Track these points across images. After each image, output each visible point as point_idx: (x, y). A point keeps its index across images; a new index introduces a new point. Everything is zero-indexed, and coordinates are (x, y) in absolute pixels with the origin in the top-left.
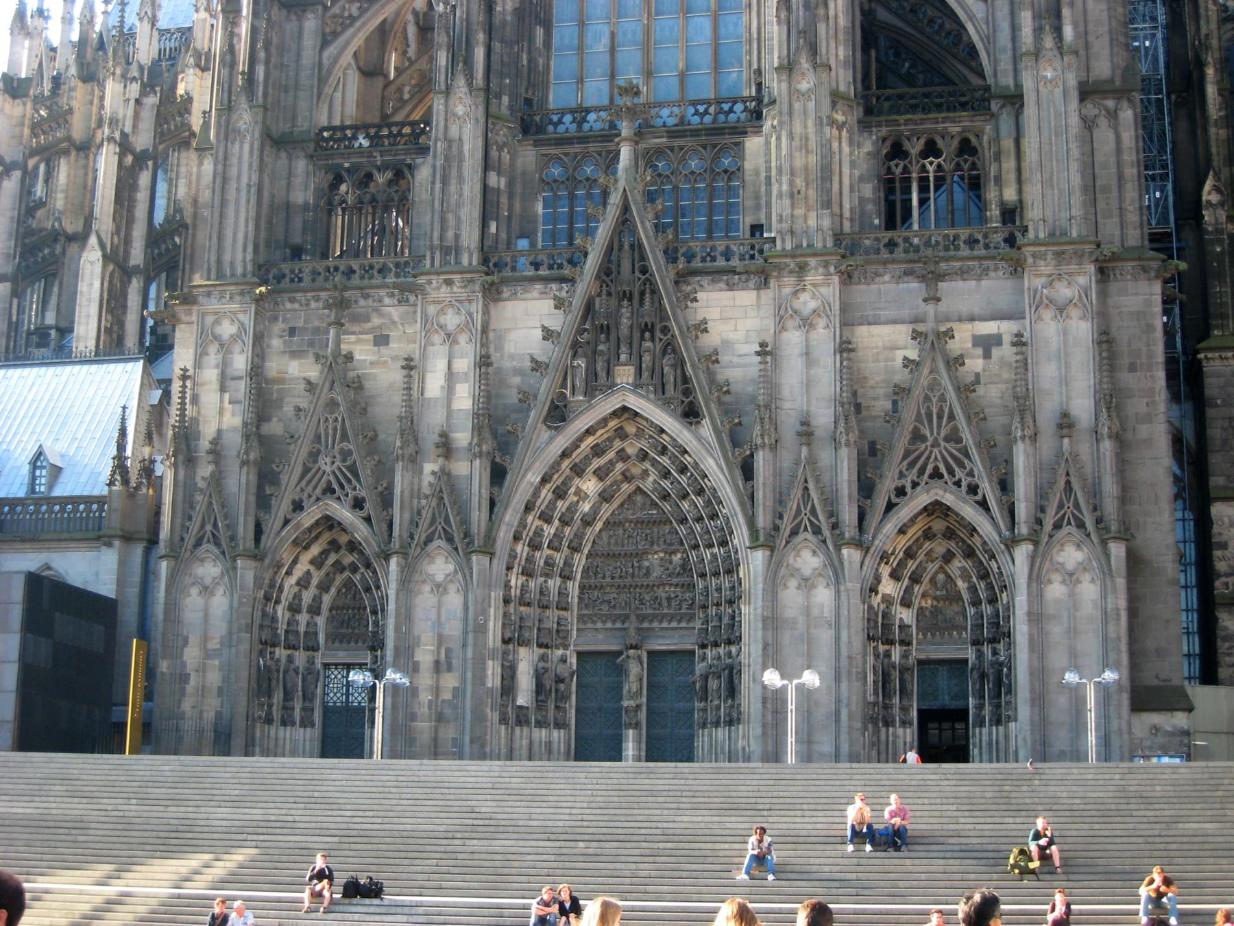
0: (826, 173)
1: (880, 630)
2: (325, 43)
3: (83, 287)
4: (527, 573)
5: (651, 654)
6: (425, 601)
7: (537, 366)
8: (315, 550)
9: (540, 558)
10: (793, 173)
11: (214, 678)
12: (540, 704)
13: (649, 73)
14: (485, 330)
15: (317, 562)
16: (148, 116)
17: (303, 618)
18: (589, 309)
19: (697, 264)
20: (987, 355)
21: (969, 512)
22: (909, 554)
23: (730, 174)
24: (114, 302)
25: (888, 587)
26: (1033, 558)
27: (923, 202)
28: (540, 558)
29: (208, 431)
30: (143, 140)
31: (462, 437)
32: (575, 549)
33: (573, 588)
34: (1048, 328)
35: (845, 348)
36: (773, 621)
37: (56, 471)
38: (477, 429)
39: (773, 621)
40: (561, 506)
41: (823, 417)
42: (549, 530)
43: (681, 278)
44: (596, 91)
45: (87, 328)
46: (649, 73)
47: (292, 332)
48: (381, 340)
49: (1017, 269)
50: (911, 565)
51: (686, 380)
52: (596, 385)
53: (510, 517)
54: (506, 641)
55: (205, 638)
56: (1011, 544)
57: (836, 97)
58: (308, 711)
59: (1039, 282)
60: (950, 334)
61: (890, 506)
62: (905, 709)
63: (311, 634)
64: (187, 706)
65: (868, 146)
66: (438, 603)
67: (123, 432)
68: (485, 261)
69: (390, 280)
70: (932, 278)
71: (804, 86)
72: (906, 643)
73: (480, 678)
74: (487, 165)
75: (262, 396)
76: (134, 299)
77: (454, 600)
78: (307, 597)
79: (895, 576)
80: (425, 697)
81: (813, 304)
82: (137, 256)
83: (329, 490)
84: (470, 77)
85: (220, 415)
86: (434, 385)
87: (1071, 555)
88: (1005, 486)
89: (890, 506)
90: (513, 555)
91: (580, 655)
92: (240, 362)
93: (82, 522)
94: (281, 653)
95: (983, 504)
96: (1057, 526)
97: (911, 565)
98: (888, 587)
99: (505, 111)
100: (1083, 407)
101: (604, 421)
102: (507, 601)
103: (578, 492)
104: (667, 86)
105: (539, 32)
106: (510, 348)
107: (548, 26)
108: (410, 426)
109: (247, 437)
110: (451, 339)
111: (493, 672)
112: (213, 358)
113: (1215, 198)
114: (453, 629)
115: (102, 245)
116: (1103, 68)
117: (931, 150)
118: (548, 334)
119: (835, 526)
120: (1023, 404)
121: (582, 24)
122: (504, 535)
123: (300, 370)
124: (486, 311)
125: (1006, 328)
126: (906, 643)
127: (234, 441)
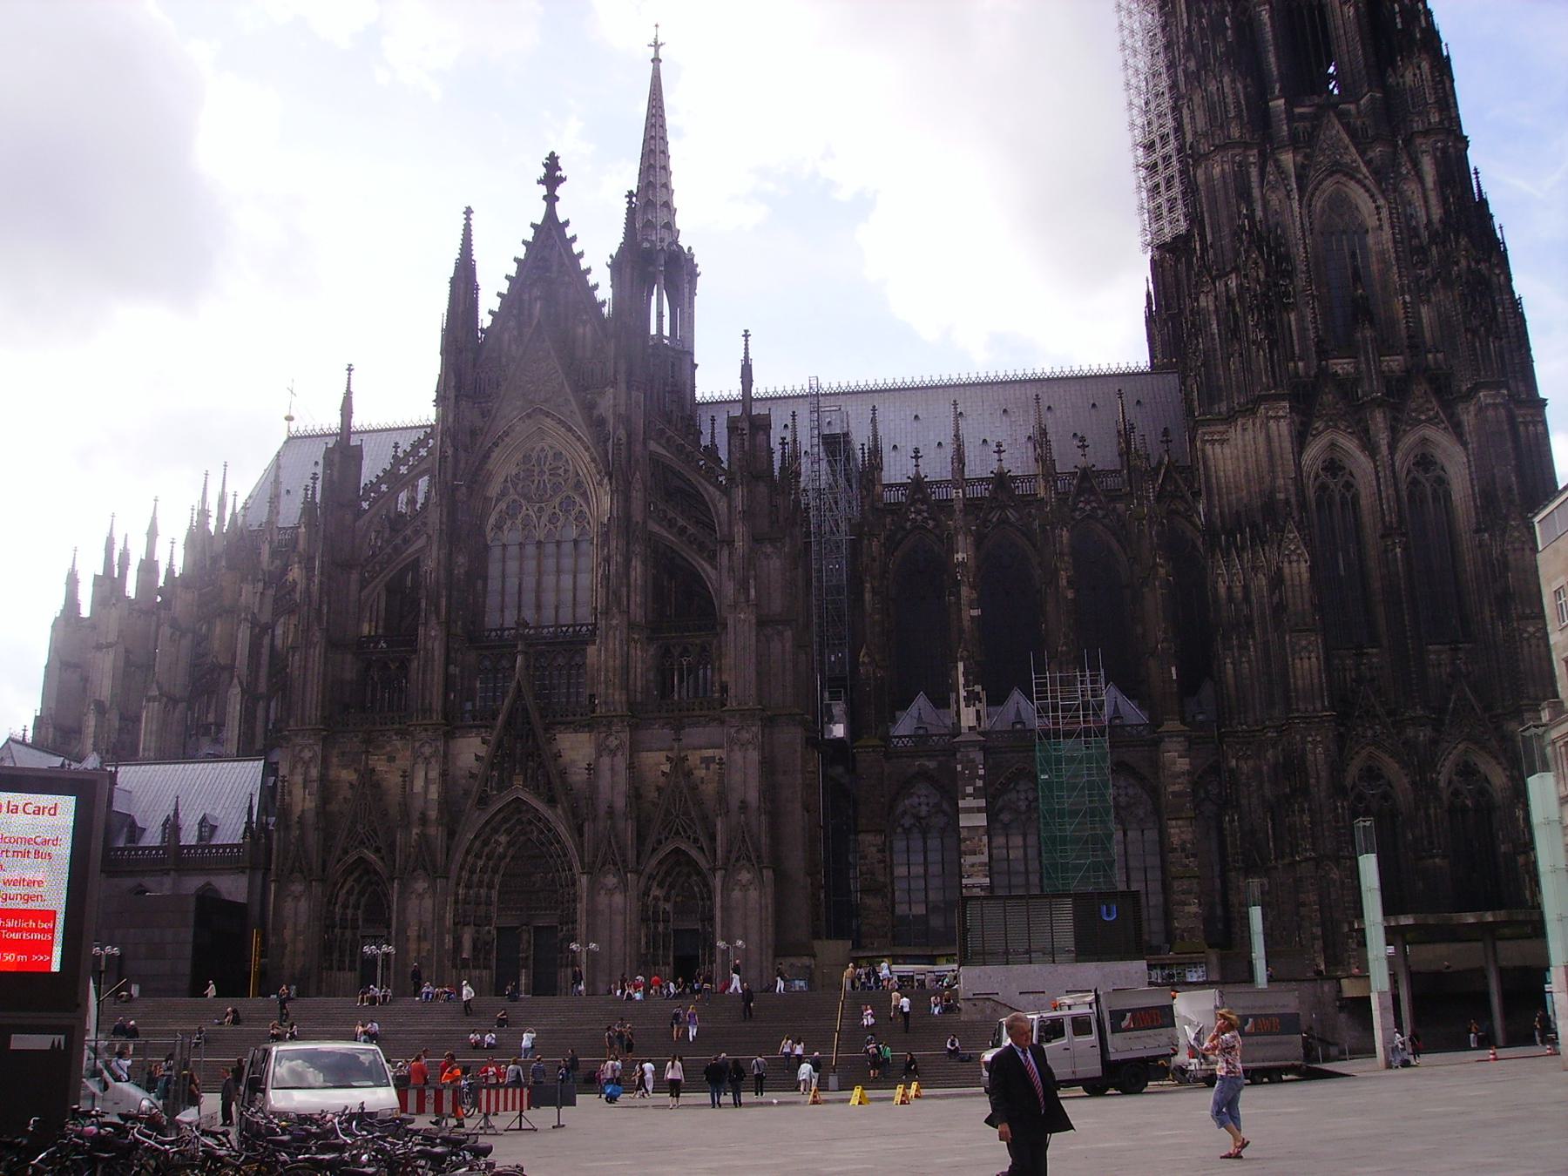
0: (626, 669)
1: (648, 916)
2: (362, 588)
3: (229, 709)
4: (468, 887)
5: (537, 929)
6: (413, 904)
7: (473, 776)
8: (356, 875)
9: (475, 878)
10: (607, 670)
11: (301, 946)
12: (475, 958)
13: (539, 607)
14: (445, 756)
15: (357, 880)
16: (268, 601)
17: (350, 912)
18: (499, 745)
19: (559, 719)
20: (707, 768)
21: (694, 853)
22: (667, 874)
23: (579, 666)
24: (248, 717)
25: (656, 891)
26: (724, 877)
27: (681, 681)
28: (475, 878)
29: (297, 811)
30: (265, 617)
31: (433, 814)
32: (495, 871)
33: (494, 894)
34: (738, 755)
35: (631, 767)
36: (592, 912)
37: (214, 828)
38: (440, 811)
39: (592, 912)
40: (487, 850)
41: (620, 803)
42: (481, 863)
43: (546, 730)
44: (510, 619)
45: (232, 731)
46: (539, 607)
47: (343, 754)
48: (391, 759)
49: (722, 722)
50: (670, 879)
51: (549, 783)
52: (503, 785)
53: (459, 857)
54: (456, 924)
55: (295, 925)
56: (714, 870)
57: (631, 626)
58: (353, 962)
59: (733, 731)
60: (685, 759)
61: (654, 850)
62: (666, 956)
63: (355, 920)
64: (286, 962)
65: (652, 651)
66: (420, 906)
67: (251, 808)
68: (445, 717)
69: (396, 726)
70: (678, 728)
71: (614, 622)
72: (666, 921)
73: (441, 942)
74: (448, 661)
75: (326, 790)
76: (260, 713)
77: (428, 902)
78: (352, 900)
79: (661, 885)
80: (413, 954)
81: (616, 742)
82: (263, 687)
83: (362, 842)
84: (438, 614)
85: (303, 801)
86: (419, 785)
87: (745, 876)
88: (713, 838)
89: (654, 850)
90: (460, 878)
91: (498, 929)
92: (314, 772)
93: (227, 860)
94: (337, 930)
95: (701, 849)
96: (738, 860)
97: (670, 879)
98: (656, 891)
99: (459, 631)
100: (753, 796)
101: (509, 804)
102: (456, 902)
103: (498, 843)
104: (548, 614)
105: (480, 583)
106: (459, 764)
107: (485, 579)
108: (405, 809)
109: (317, 814)
110: (427, 761)
111: (448, 939)
112: (300, 769)
113: (866, 660)
114: (428, 917)
115: (241, 683)
116: (777, 605)
117: (685, 652)
118: (478, 758)
119: (624, 861)
120: (722, 797)
121: (504, 576)
122: (455, 867)
123: (348, 775)
124: (446, 743)
125: (717, 753)
126: (666, 921)
127: (310, 818)
